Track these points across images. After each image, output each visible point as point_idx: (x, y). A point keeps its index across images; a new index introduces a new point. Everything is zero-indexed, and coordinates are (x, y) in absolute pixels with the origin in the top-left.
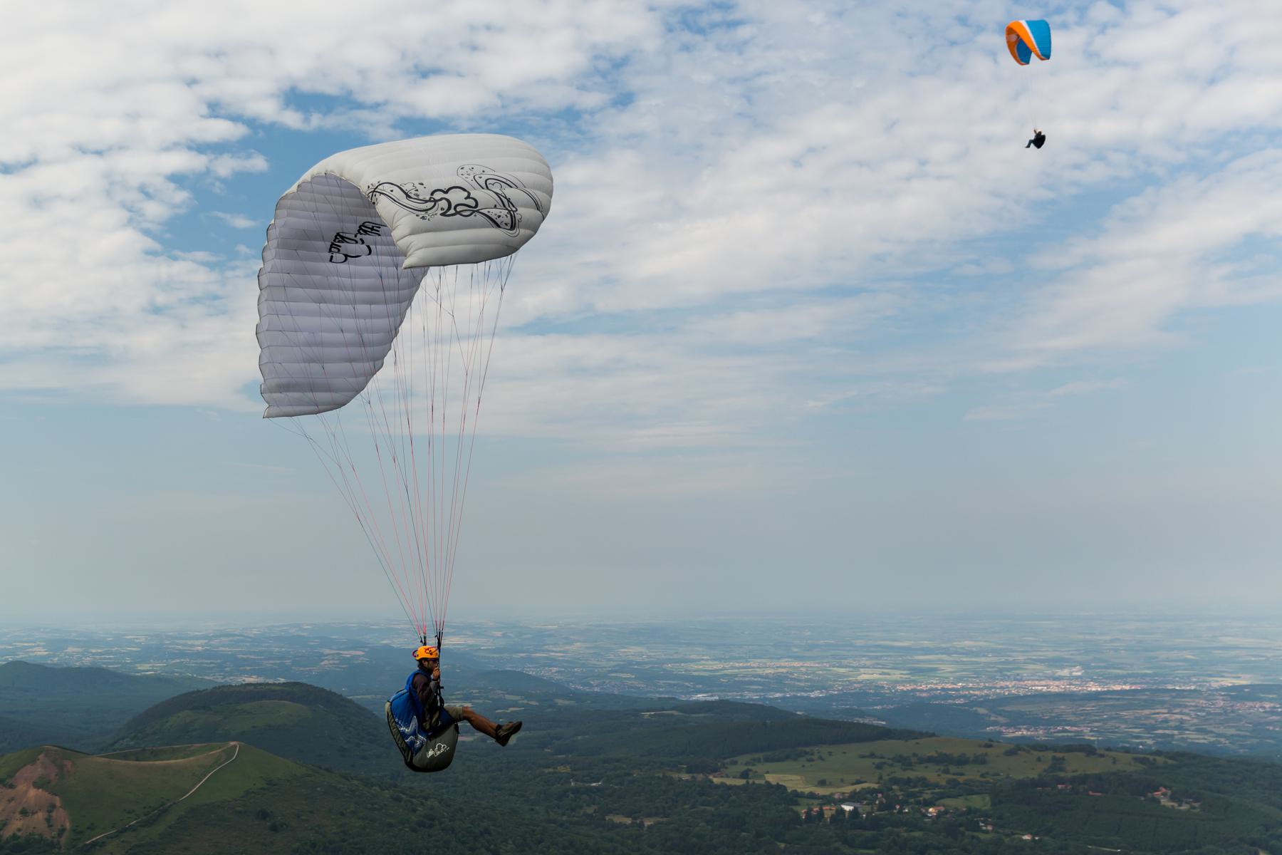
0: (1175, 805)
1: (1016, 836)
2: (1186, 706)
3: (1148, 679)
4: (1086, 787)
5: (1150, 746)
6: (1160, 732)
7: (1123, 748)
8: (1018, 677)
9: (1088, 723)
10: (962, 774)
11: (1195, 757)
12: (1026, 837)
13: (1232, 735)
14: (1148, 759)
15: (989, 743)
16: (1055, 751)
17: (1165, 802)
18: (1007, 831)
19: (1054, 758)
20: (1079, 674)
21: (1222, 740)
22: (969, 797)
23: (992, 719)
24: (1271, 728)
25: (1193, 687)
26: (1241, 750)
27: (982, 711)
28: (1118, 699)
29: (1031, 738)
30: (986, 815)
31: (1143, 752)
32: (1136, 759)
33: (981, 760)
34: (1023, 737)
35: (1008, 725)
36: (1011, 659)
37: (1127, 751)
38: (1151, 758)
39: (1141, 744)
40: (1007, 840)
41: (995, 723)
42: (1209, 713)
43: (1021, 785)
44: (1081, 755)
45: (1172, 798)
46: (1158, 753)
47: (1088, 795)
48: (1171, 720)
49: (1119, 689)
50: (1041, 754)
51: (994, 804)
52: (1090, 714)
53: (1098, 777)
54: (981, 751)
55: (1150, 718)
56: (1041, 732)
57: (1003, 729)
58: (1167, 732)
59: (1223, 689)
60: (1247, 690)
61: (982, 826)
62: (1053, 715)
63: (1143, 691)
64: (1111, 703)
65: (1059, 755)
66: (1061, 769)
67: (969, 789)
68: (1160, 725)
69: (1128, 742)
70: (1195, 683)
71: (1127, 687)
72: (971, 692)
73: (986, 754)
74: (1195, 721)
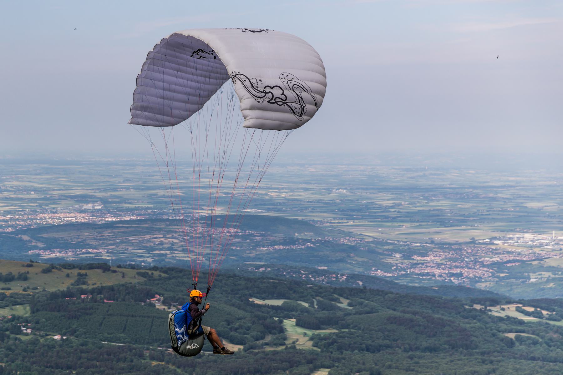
0: (166, 308)
1: (49, 337)
2: (176, 232)
3: (149, 211)
4: (102, 296)
5: (150, 264)
6: (157, 252)
7: (130, 265)
8: (54, 211)
9: (105, 246)
10: (9, 289)
11: (181, 271)
12: (57, 337)
13: (207, 254)
14: (148, 273)
15: (31, 263)
16: (80, 269)
17: (159, 306)
18: (42, 333)
19: (79, 274)
20: (100, 207)
21: (201, 257)
22: (14, 307)
23: (33, 244)
24: (234, 248)
25: (181, 217)
26: (213, 265)
27: (25, 238)
28: (127, 227)
29: (62, 259)
30: (27, 321)
31: (145, 268)
32: (138, 274)
33: (24, 277)
34: (57, 258)
35: (45, 249)
36: (48, 196)
37: (133, 267)
38: (150, 272)
39: (143, 261)
40: (42, 340)
41: (36, 247)
42: (192, 237)
43: (54, 296)
44: (99, 271)
45: (164, 303)
46: (155, 268)
47: (104, 303)
48: (165, 243)
49: (129, 219)
50: (69, 271)
51: (33, 312)
52: (107, 239)
53: (112, 289)
54: (23, 270)
55: (150, 241)
56: (70, 254)
57: (41, 252)
58: (162, 252)
59: (202, 218)
60: (218, 219)
61: (24, 330)
62: (80, 240)
63: (145, 221)
64: (122, 230)
65: (83, 272)
66: (84, 283)
67: (14, 301)
68: (157, 247)
69: (134, 261)
70: (183, 214)
71: (134, 218)
72: (17, 223)
73: (28, 273)
74: (183, 243)
